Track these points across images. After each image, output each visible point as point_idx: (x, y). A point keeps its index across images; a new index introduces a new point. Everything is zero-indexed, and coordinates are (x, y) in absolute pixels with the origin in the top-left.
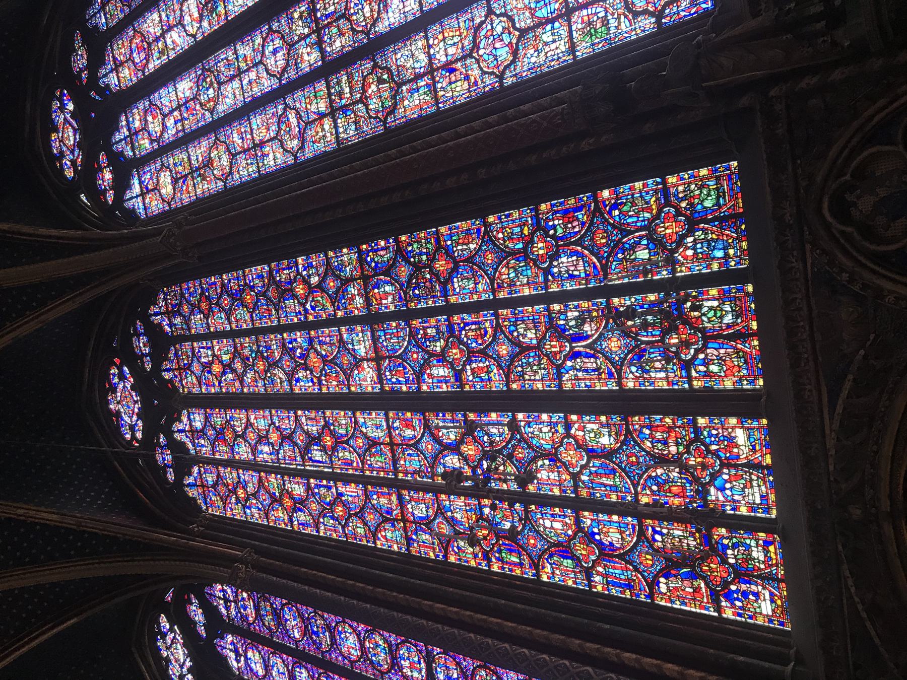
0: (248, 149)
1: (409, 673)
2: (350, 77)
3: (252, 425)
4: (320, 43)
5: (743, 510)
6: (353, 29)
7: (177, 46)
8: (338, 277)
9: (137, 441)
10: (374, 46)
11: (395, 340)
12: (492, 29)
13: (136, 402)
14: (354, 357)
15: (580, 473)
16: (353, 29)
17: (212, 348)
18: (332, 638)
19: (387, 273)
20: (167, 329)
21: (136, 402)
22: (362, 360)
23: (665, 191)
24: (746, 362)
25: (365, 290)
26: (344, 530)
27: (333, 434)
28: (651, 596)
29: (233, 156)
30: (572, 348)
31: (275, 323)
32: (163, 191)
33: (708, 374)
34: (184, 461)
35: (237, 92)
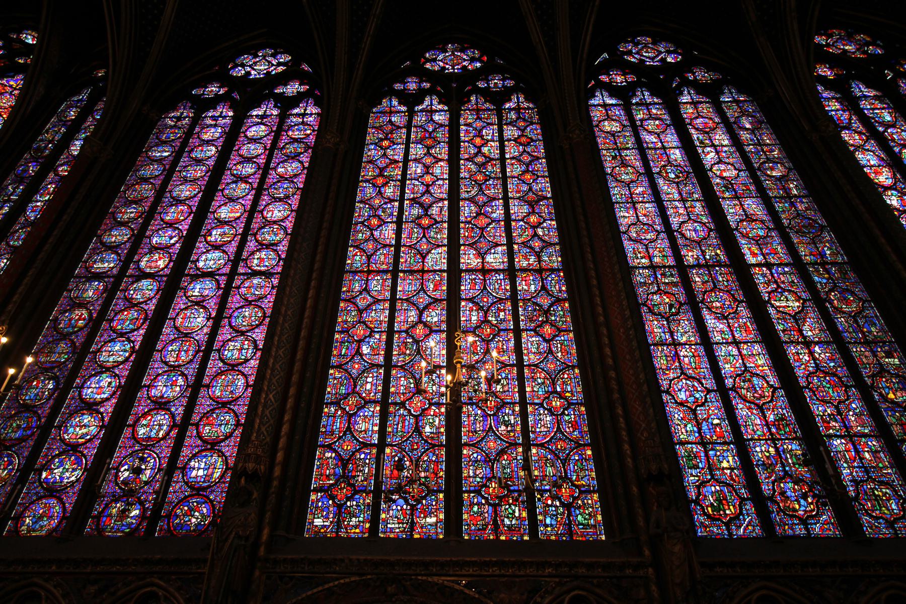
0: (632, 198)
1: (256, 257)
2: (675, 284)
3: (437, 162)
4: (699, 266)
5: (383, 516)
6: (705, 292)
8: (542, 251)
9: (425, 63)
10: (694, 305)
11: (497, 287)
12: (698, 391)
13: (453, 69)
14: (486, 253)
15: (406, 409)
16: (705, 292)
17: (492, 140)
18: (280, 200)
19: (544, 288)
20: (507, 106)
21: (453, 69)
22: (483, 259)
23: (589, 492)
24: (479, 529)
25: (532, 269)
26: (360, 223)
27: (430, 227)
28: (323, 446)
29: (628, 185)
30: (490, 415)
31: (510, 195)
32: (606, 123)
33: (472, 505)
34: (411, 100)
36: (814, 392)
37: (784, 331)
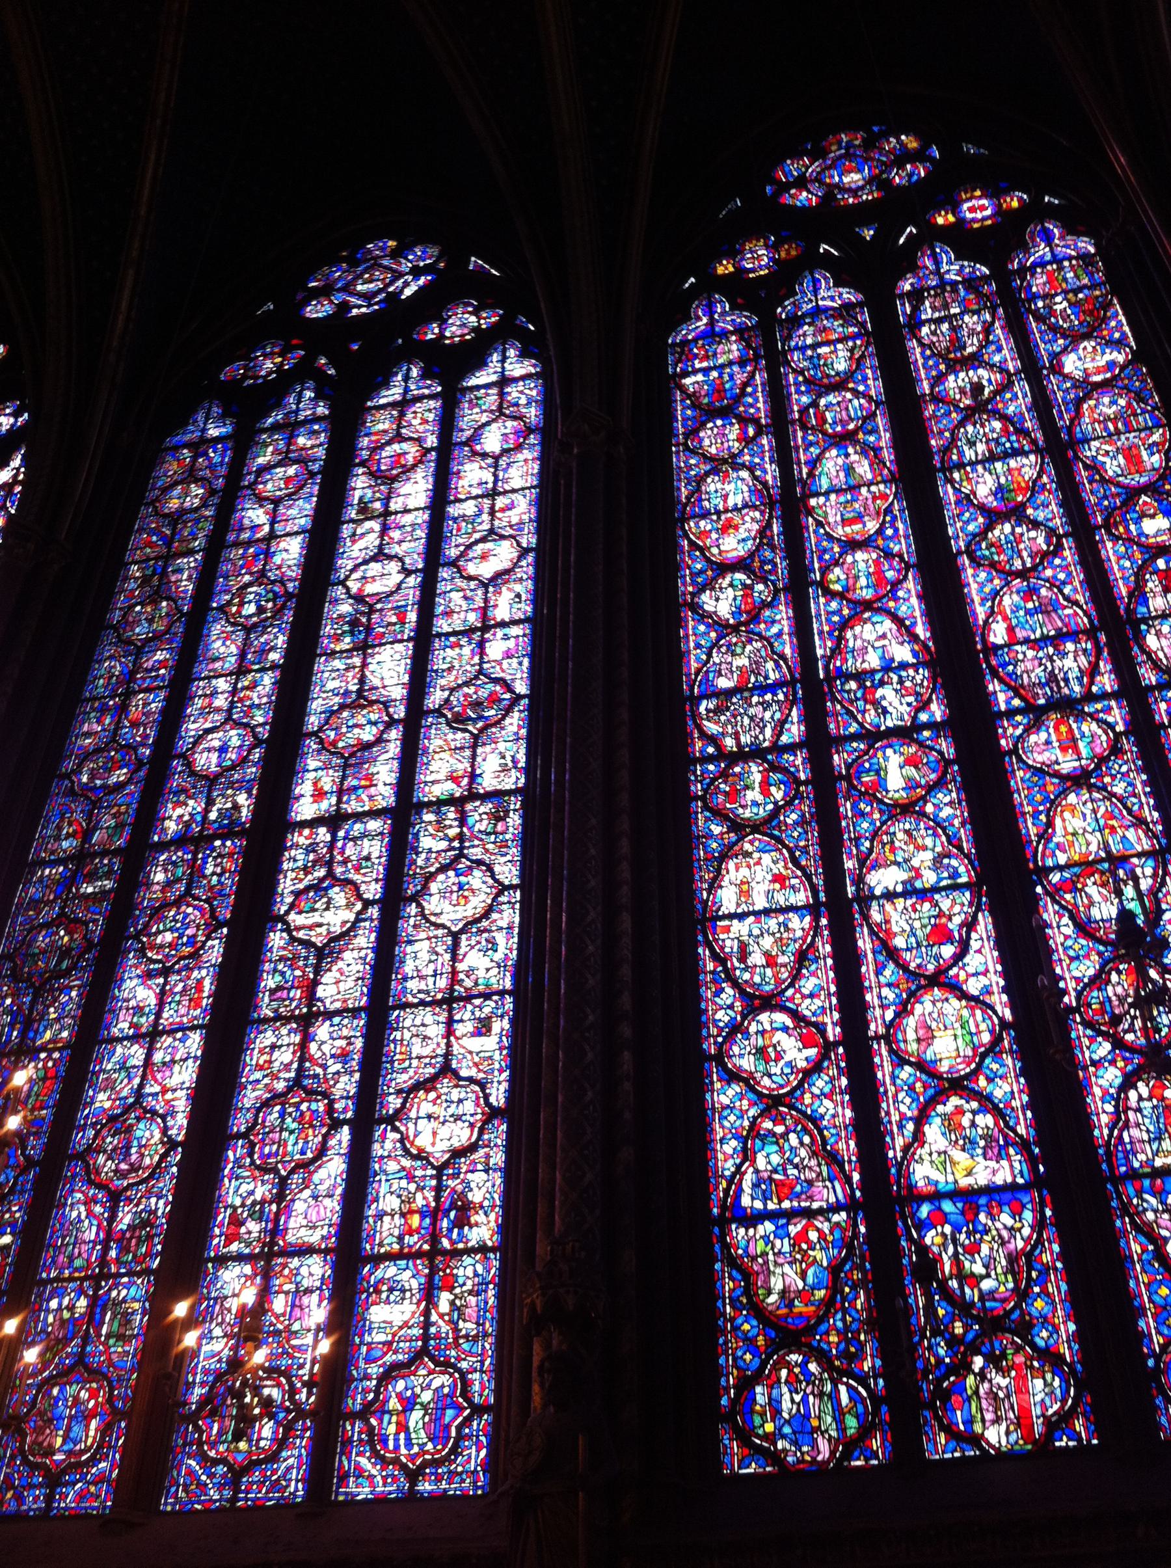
7: (354, 542)
35: (218, 665)
36: (252, 1145)
37: (273, 992)
